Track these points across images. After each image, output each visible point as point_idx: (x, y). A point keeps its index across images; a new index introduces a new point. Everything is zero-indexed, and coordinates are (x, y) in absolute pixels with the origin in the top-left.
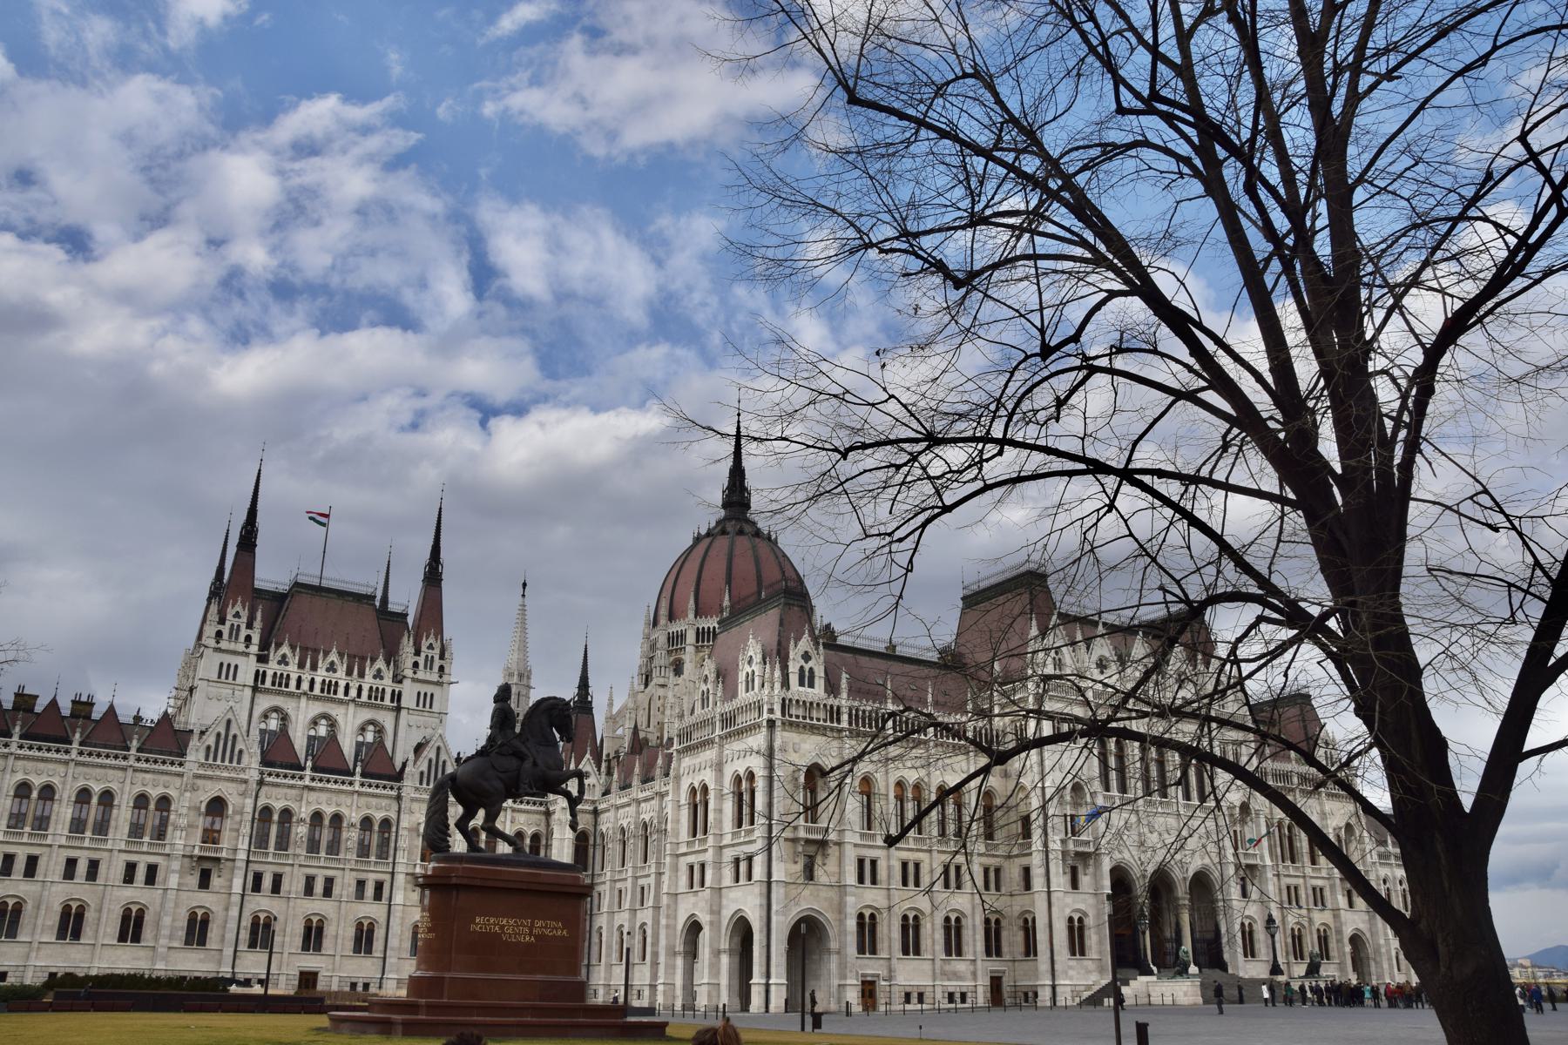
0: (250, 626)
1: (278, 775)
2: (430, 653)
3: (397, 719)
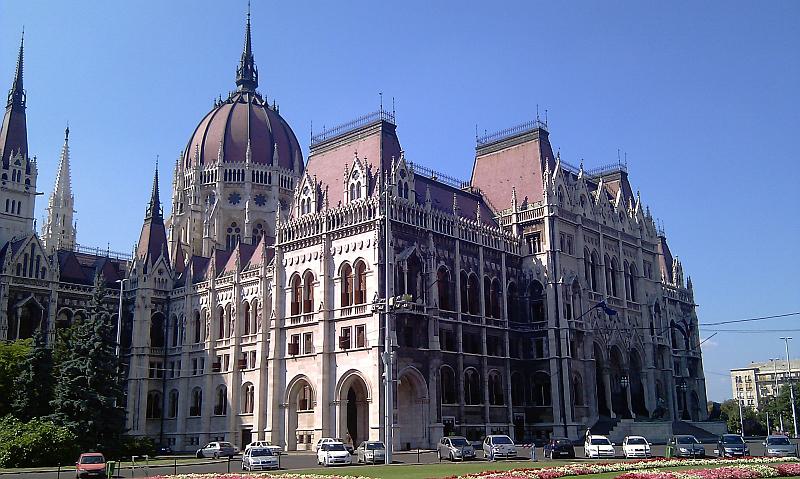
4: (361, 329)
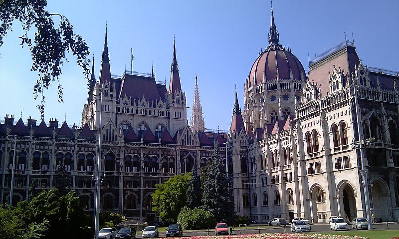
0: (111, 91)
1: (131, 144)
2: (178, 97)
4: (346, 158)
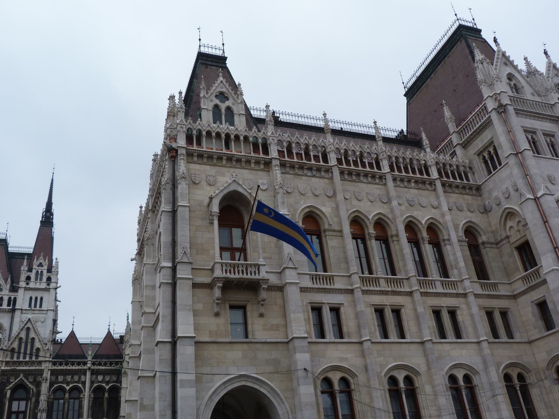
3: (12, 318)
